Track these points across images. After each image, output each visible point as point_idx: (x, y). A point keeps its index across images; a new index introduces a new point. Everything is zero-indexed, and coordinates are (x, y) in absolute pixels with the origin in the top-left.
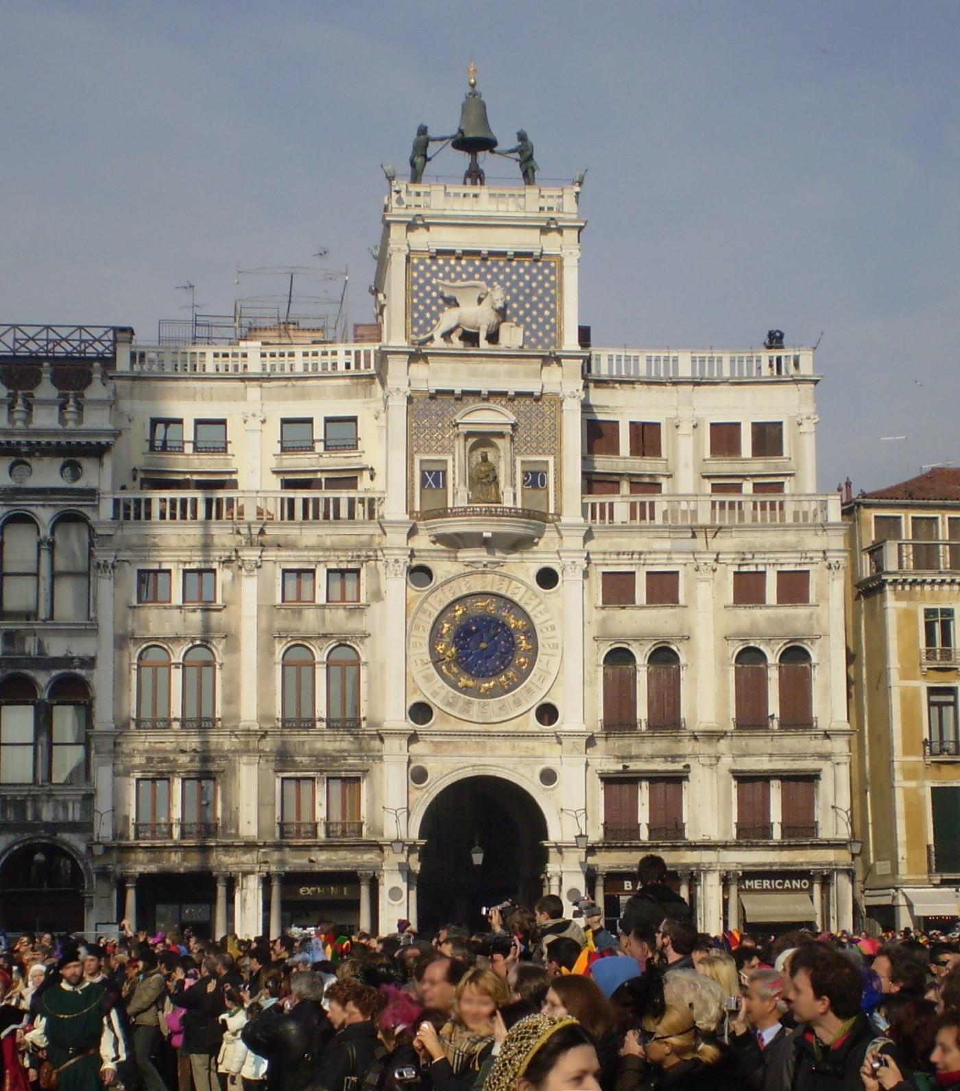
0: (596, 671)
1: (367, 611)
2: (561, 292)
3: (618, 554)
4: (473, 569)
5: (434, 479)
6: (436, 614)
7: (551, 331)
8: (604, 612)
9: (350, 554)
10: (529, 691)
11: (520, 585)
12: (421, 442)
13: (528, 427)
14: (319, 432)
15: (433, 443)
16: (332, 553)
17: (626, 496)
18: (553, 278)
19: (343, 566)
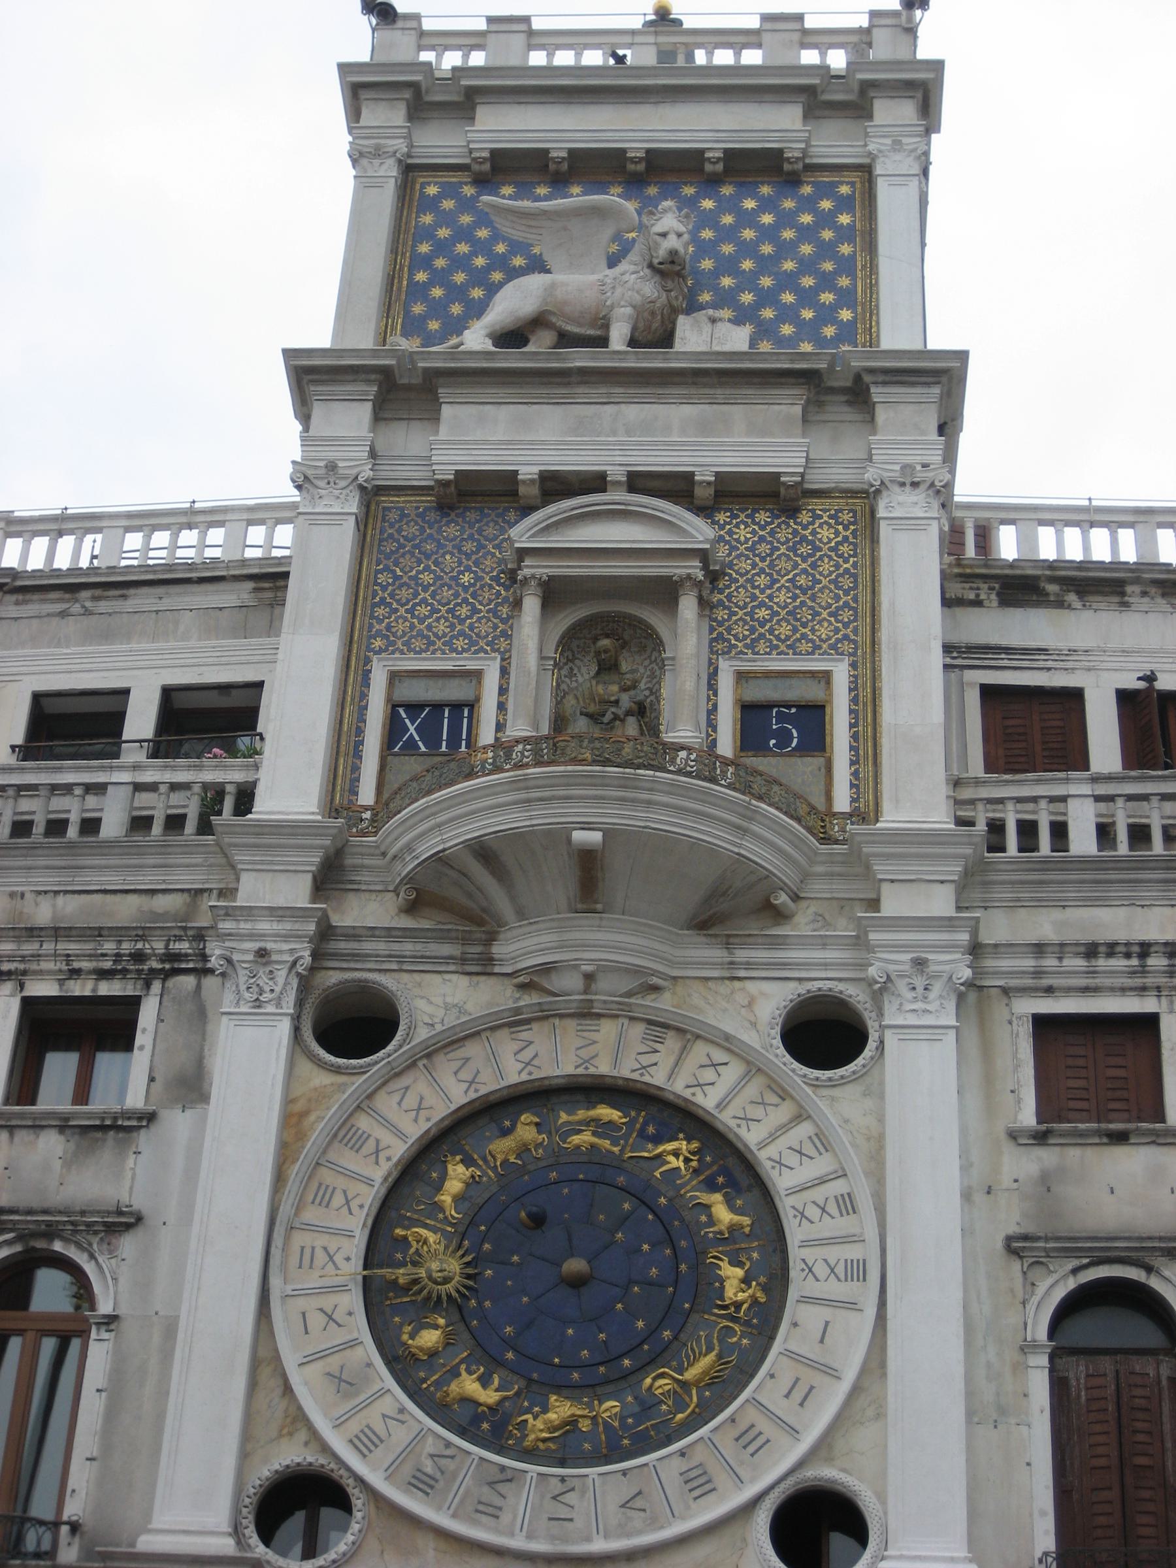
0: (1020, 1368)
1: (143, 1138)
2: (871, 247)
3: (1091, 951)
4: (541, 999)
5: (431, 729)
6: (399, 1150)
7: (838, 339)
8: (1047, 1156)
9: (109, 946)
10: (749, 1439)
11: (719, 1056)
12: (401, 627)
13: (762, 581)
14: (141, 721)
15: (442, 627)
16: (48, 946)
17: (1109, 778)
18: (844, 219)
19: (81, 988)
